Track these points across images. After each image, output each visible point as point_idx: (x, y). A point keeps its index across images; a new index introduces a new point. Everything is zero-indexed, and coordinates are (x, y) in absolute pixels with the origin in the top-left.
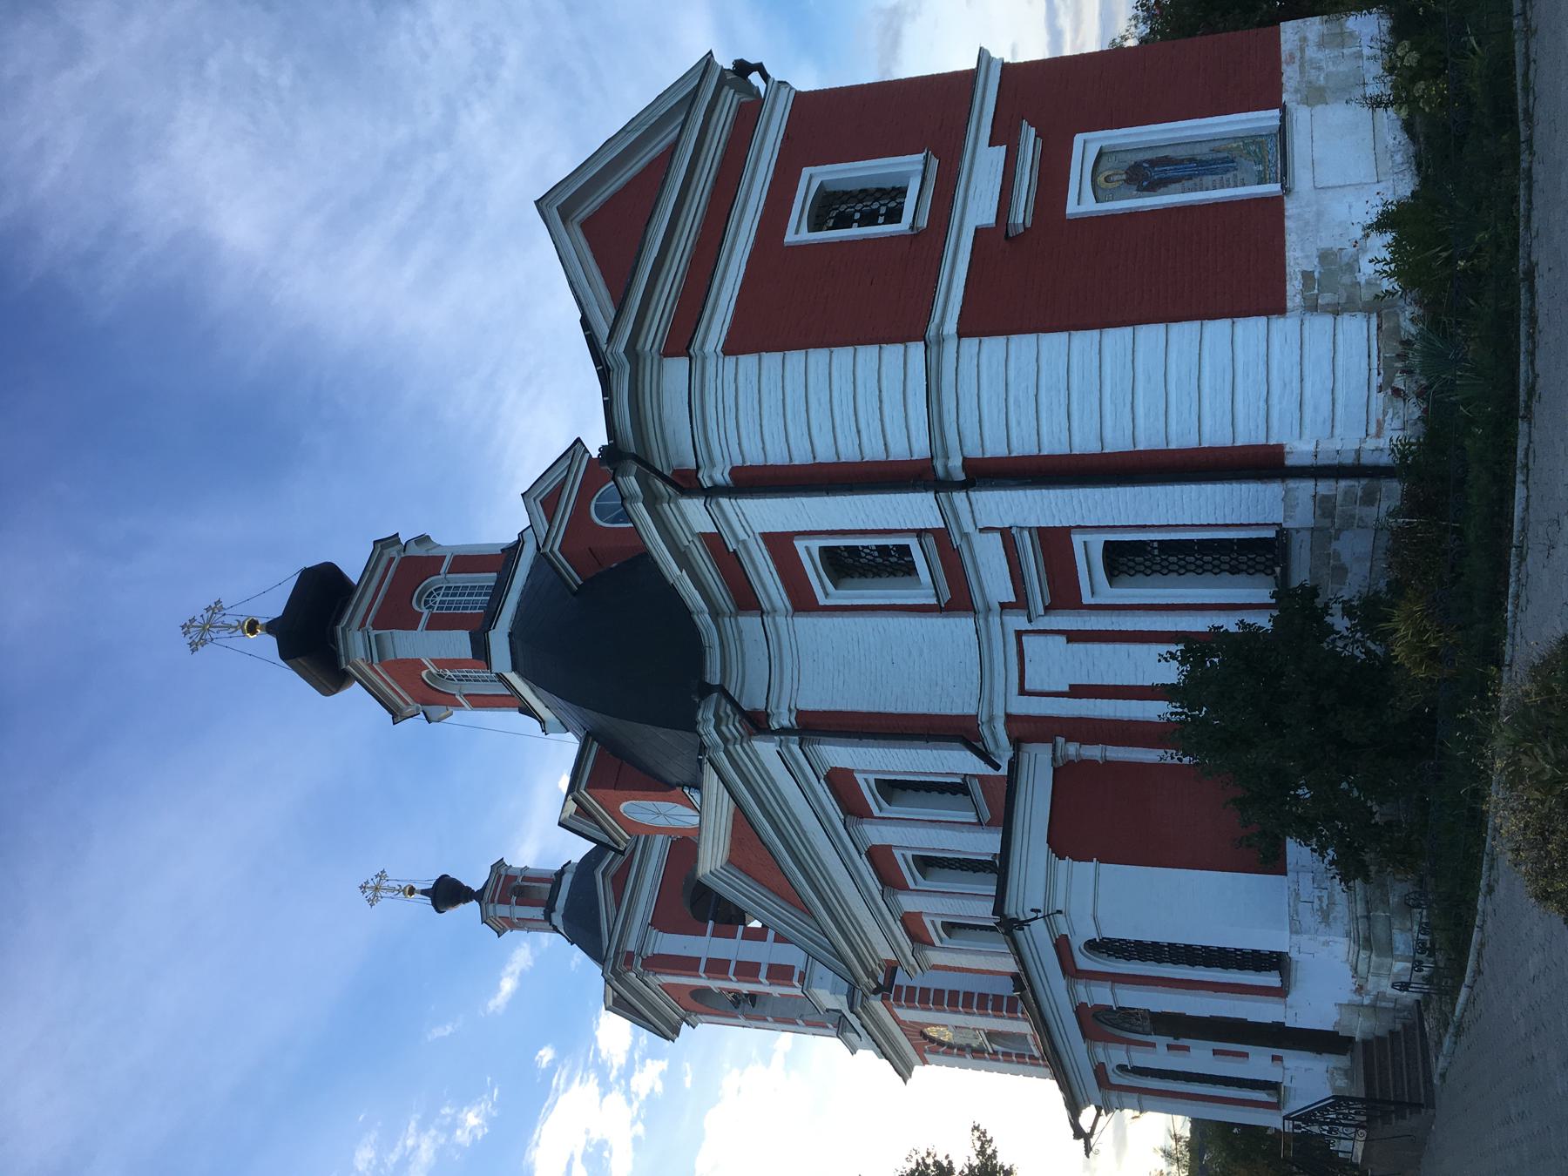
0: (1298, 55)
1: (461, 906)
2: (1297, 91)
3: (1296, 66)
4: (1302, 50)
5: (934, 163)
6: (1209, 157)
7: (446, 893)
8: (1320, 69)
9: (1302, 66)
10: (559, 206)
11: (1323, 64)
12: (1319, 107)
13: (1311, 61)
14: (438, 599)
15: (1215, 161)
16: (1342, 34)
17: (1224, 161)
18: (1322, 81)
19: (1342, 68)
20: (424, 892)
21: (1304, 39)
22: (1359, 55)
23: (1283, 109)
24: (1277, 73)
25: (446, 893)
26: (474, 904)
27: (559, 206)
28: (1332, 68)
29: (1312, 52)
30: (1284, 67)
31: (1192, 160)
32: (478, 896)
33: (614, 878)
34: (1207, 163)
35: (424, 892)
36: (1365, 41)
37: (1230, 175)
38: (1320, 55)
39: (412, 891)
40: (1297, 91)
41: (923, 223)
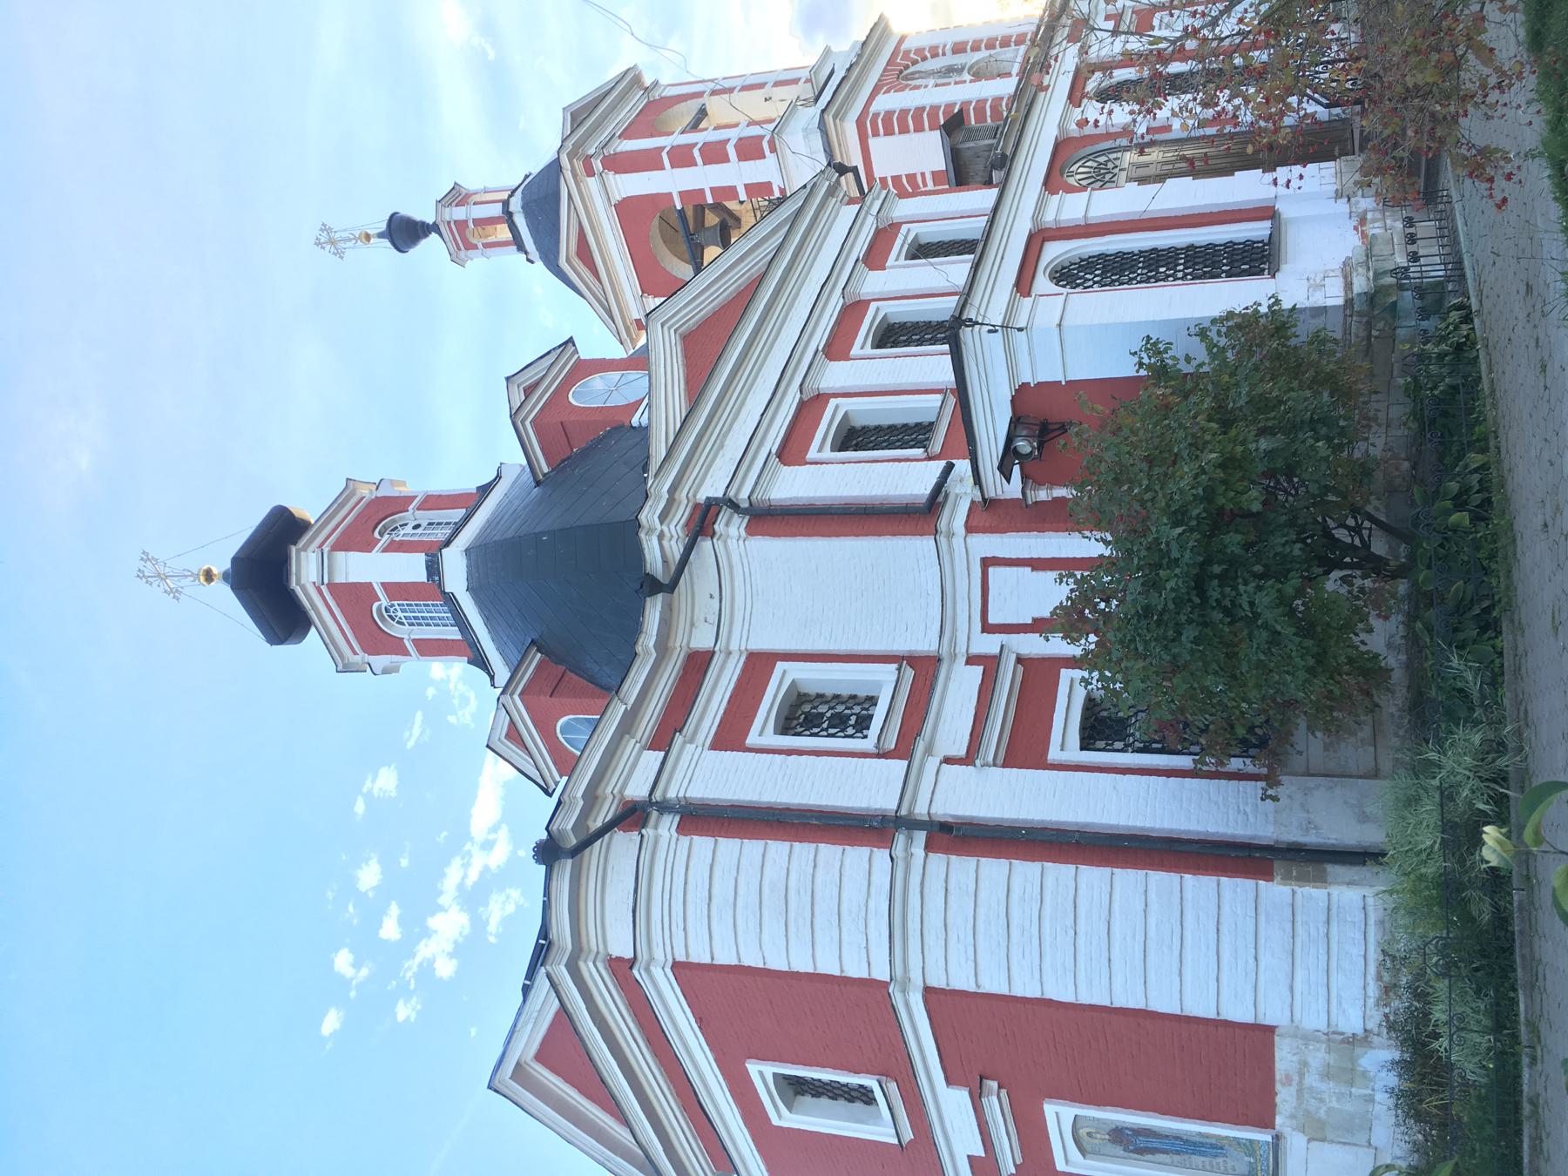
0: (1296, 1078)
1: (424, 243)
2: (1293, 1117)
3: (1293, 1089)
4: (1301, 1075)
5: (892, 1087)
6: (1197, 1139)
7: (404, 232)
8: (1321, 1100)
9: (1300, 1091)
10: (511, 1080)
11: (1326, 1096)
12: (1314, 1144)
13: (1311, 1088)
14: (400, 614)
15: (1202, 1145)
16: (1353, 1070)
17: (1213, 1146)
18: (1322, 1113)
19: (1349, 1107)
20: (381, 235)
21: (1305, 1064)
22: (1370, 1100)
23: (1277, 1138)
24: (1272, 1094)
25: (404, 232)
26: (434, 236)
27: (511, 1080)
28: (1335, 1104)
29: (1311, 1080)
30: (1278, 1087)
31: (1177, 1138)
32: (435, 227)
33: (579, 254)
34: (1194, 1144)
35: (381, 235)
36: (1379, 1085)
37: (1220, 1160)
38: (1323, 1086)
39: (368, 237)
40: (1293, 1117)
41: (908, 1135)
